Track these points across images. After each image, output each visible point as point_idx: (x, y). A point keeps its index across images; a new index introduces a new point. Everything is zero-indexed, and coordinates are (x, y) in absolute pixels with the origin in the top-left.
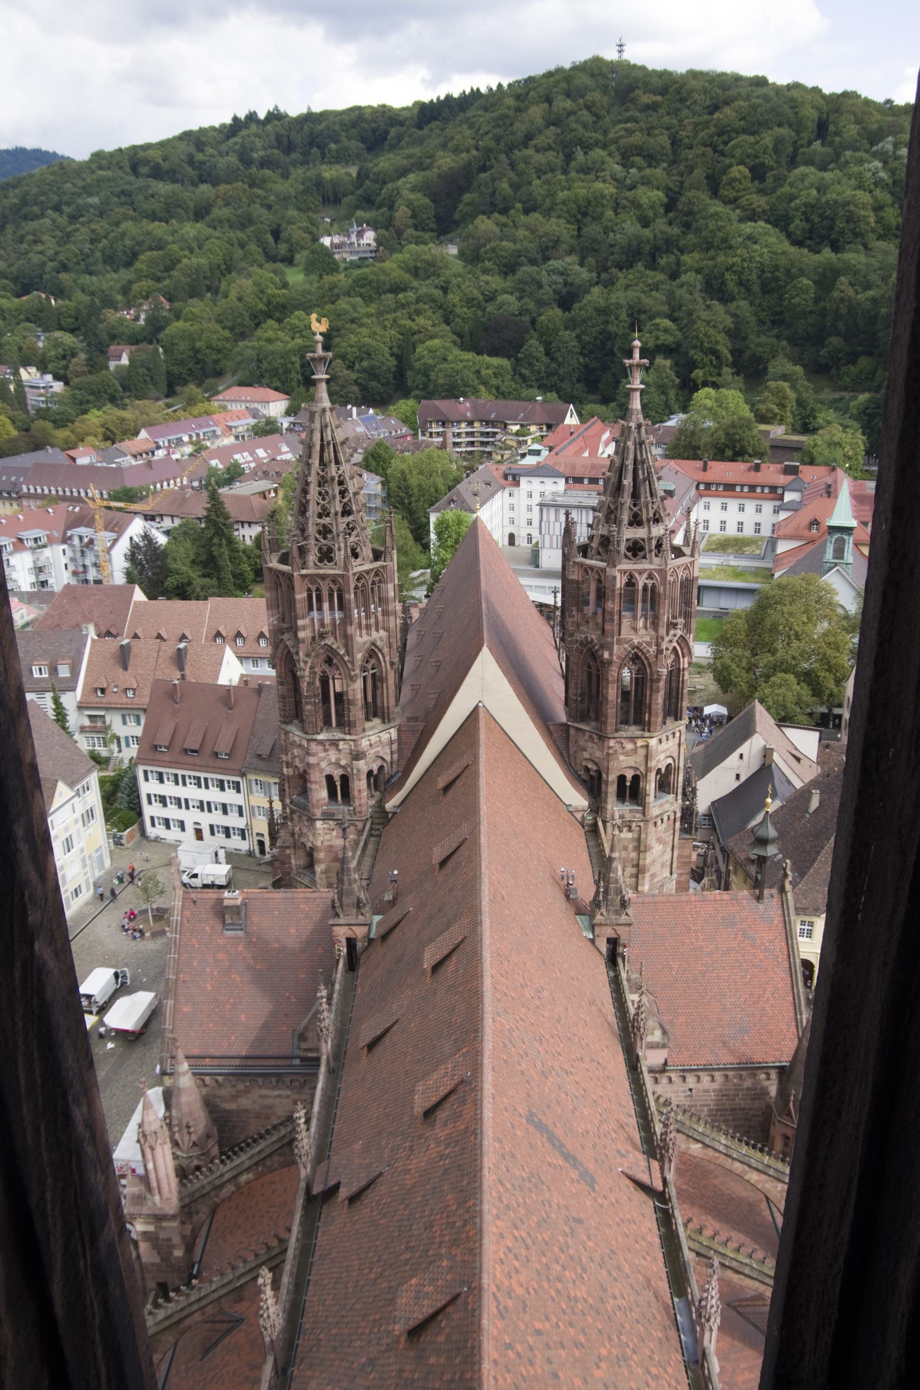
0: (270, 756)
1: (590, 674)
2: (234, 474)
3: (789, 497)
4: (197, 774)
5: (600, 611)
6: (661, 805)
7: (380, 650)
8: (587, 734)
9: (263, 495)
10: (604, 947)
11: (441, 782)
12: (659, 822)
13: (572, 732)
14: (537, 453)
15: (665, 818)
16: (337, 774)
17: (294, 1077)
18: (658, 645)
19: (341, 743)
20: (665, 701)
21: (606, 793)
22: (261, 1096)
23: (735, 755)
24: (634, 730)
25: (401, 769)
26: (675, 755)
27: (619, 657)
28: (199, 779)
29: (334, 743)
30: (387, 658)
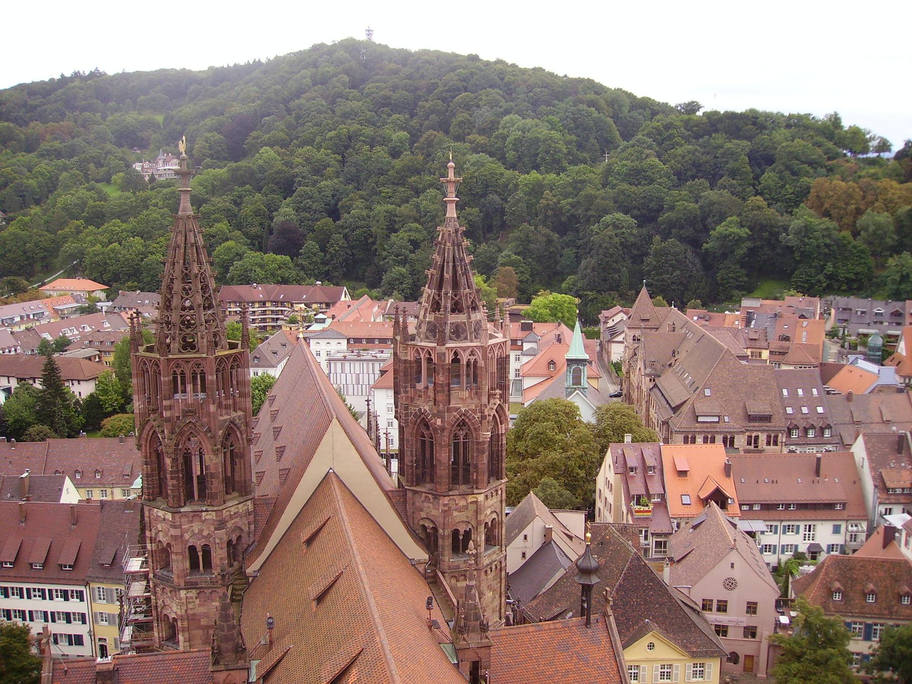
1: (423, 442)
3: (526, 346)
4: (41, 586)
5: (431, 386)
6: (490, 555)
7: (238, 428)
8: (424, 495)
9: (89, 359)
10: (466, 668)
11: (305, 535)
13: (409, 494)
15: (494, 567)
16: (199, 544)
18: (482, 412)
19: (204, 514)
21: (443, 547)
23: (521, 536)
24: (463, 488)
25: (257, 539)
27: (449, 424)
28: (43, 591)
29: (196, 514)
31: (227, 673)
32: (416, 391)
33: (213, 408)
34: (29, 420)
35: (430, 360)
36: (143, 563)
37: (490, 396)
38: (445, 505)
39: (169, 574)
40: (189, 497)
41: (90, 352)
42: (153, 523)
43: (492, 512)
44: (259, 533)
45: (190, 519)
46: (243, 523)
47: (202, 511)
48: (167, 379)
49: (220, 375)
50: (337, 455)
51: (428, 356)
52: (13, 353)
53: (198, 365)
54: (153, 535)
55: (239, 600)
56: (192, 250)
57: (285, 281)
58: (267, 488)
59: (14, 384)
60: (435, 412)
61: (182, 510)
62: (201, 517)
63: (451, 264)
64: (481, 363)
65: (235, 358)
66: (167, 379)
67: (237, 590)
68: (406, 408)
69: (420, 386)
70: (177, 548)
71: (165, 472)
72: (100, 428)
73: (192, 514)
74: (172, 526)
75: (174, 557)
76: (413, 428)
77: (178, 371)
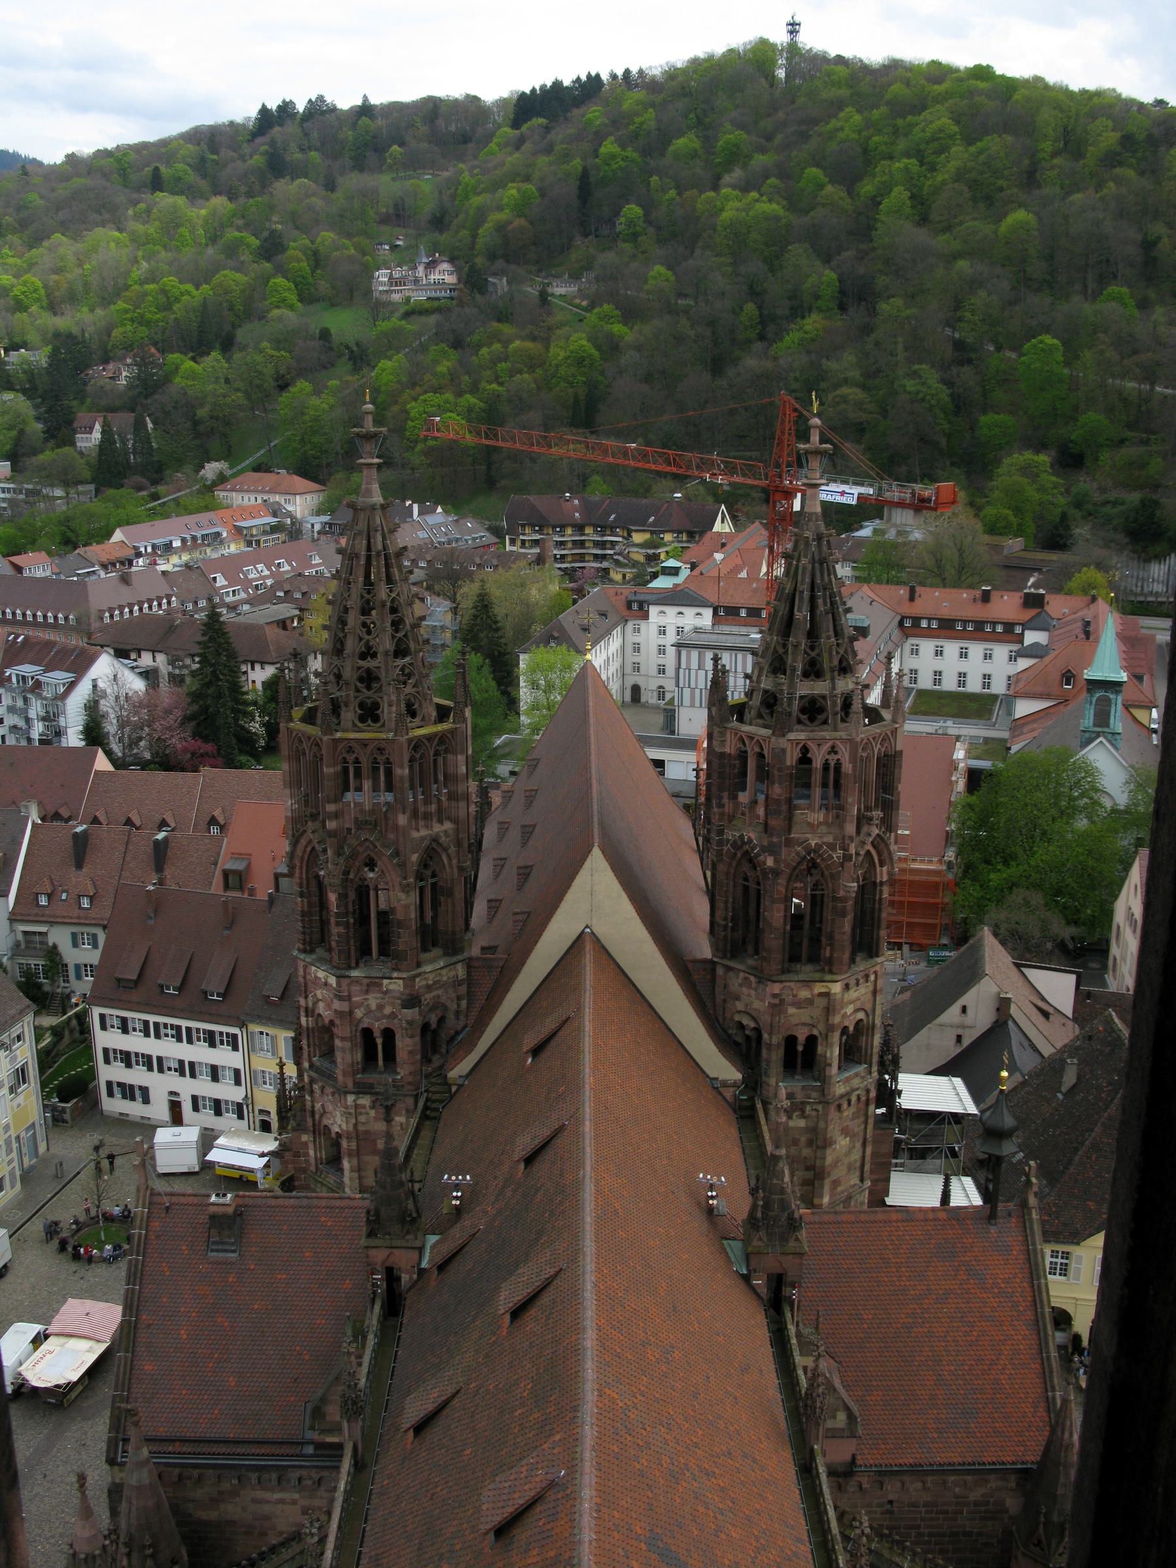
0: (282, 998)
1: (746, 889)
5: (761, 798)
6: (848, 1080)
7: (445, 850)
8: (742, 975)
9: (283, 624)
11: (530, 1040)
12: (845, 1106)
13: (720, 971)
14: (675, 572)
15: (854, 1099)
16: (377, 1027)
17: (304, 1473)
18: (845, 848)
19: (385, 982)
20: (853, 929)
21: (768, 1062)
22: (255, 1501)
23: (955, 1008)
24: (806, 970)
25: (471, 1022)
26: (868, 1007)
28: (179, 1028)
29: (373, 984)
30: (454, 861)
31: (387, 1252)
32: (737, 805)
33: (402, 820)
35: (761, 756)
37: (862, 821)
38: (775, 996)
42: (310, 985)
43: (856, 1011)
44: (474, 1014)
46: (447, 997)
48: (331, 770)
50: (596, 902)
51: (757, 749)
52: (164, 607)
53: (381, 750)
54: (310, 1005)
55: (435, 1118)
56: (378, 562)
60: (765, 843)
62: (381, 985)
63: (806, 594)
64: (847, 767)
65: (442, 738)
66: (331, 770)
67: (435, 1101)
68: (721, 832)
69: (744, 797)
70: (342, 1030)
74: (336, 996)
75: (338, 1043)
76: (730, 865)
77: (351, 758)
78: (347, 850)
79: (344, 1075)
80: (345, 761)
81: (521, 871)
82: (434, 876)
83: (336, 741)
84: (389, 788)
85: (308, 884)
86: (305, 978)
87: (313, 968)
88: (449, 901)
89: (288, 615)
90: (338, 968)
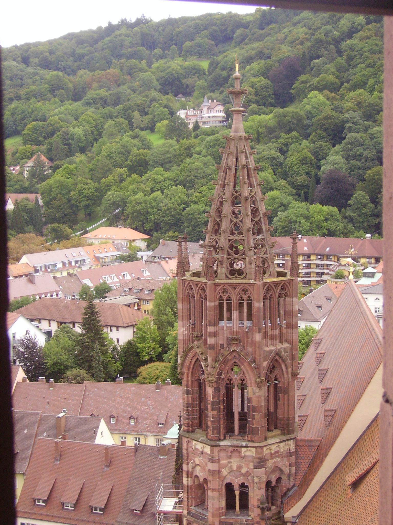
0: (142, 511)
2: (103, 291)
7: (284, 361)
9: (129, 306)
11: (351, 478)
14: (372, 275)
19: (243, 449)
25: (298, 483)
29: (236, 449)
30: (290, 370)
33: (258, 337)
34: (68, 363)
36: (176, 503)
39: (204, 512)
40: (230, 431)
41: (130, 299)
44: (300, 477)
45: (229, 454)
46: (283, 464)
47: (242, 447)
48: (212, 304)
49: (267, 302)
52: (54, 297)
54: (190, 469)
56: (243, 172)
57: (331, 234)
58: (310, 431)
59: (54, 327)
61: (222, 443)
62: (240, 452)
66: (212, 304)
70: (214, 484)
71: (206, 402)
72: (136, 376)
73: (231, 449)
74: (209, 460)
75: (210, 493)
77: (225, 297)
78: (221, 359)
79: (213, 516)
80: (221, 299)
81: (324, 391)
82: (276, 380)
83: (216, 285)
84: (250, 318)
85: (192, 385)
86: (187, 450)
87: (194, 442)
88: (286, 396)
89: (132, 302)
90: (212, 440)
